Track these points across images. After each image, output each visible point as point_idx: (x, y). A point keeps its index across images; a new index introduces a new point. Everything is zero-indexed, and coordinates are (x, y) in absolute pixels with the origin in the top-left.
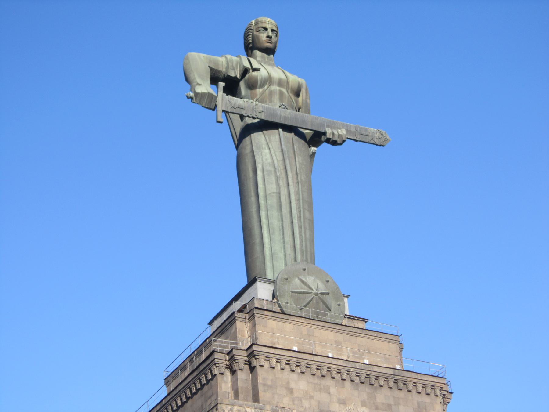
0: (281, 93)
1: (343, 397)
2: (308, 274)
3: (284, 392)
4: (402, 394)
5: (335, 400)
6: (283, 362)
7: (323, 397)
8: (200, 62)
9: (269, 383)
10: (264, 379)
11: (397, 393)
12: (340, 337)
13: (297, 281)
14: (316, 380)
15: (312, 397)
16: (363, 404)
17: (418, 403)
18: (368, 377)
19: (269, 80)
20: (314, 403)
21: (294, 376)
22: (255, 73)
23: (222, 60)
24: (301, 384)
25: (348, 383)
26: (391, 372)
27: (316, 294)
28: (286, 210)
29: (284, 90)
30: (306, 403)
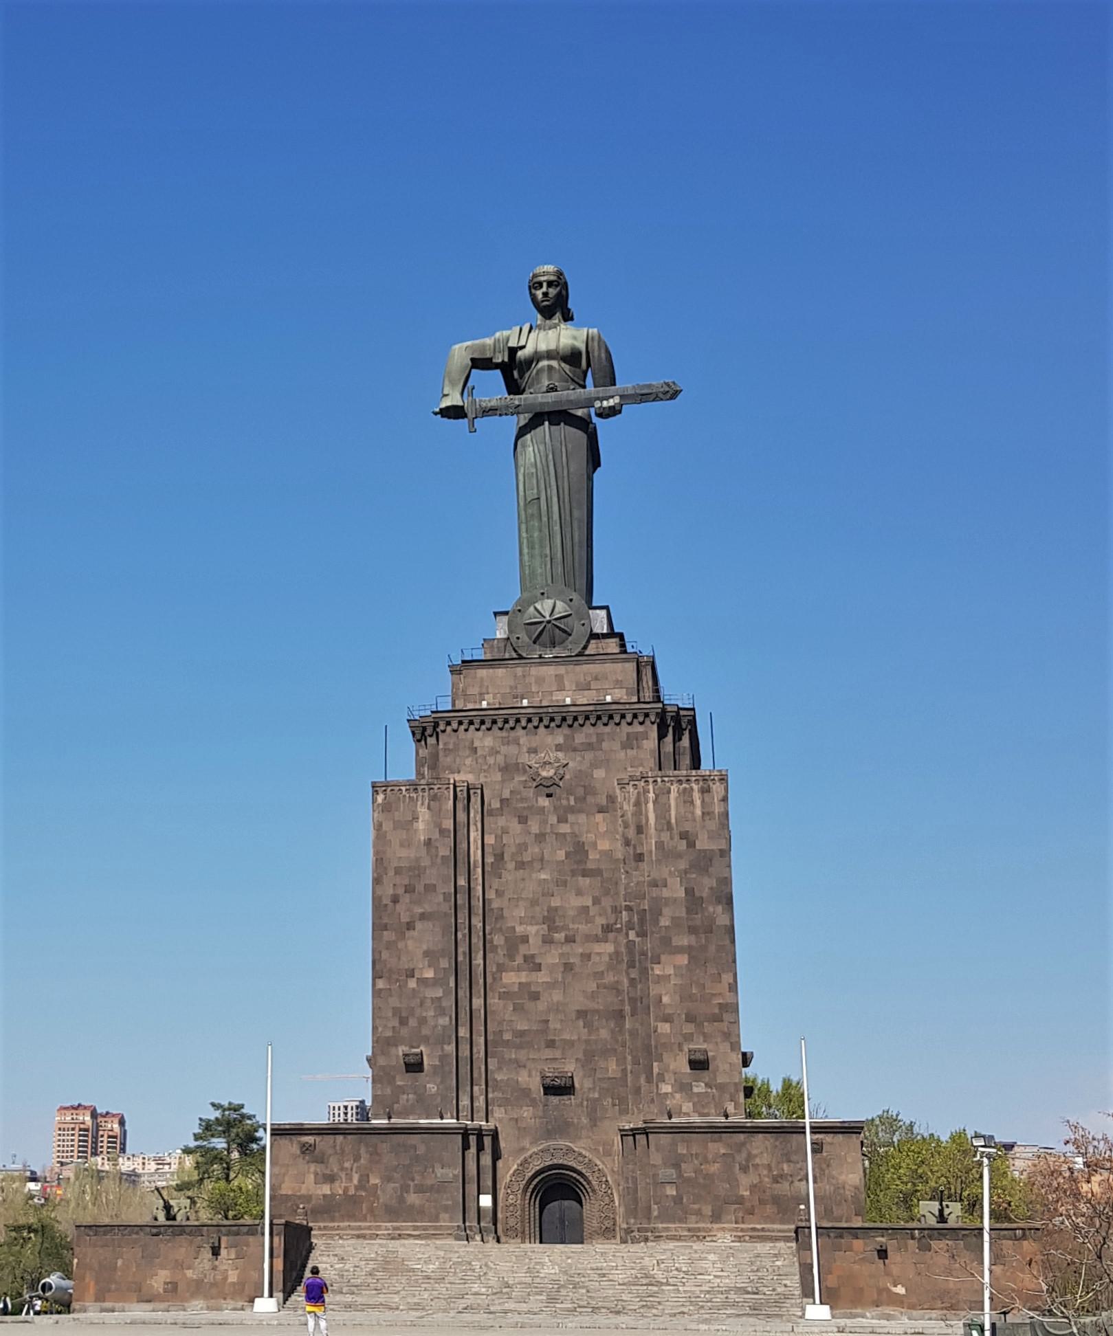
0: (550, 368)
1: (534, 745)
2: (548, 598)
3: (468, 752)
4: (607, 729)
5: (525, 749)
6: (466, 722)
7: (513, 749)
8: (460, 353)
9: (451, 747)
10: (445, 744)
11: (600, 728)
12: (561, 670)
13: (532, 609)
14: (504, 734)
15: (498, 752)
16: (559, 748)
17: (628, 734)
18: (564, 719)
19: (537, 357)
20: (500, 759)
21: (480, 733)
22: (520, 353)
23: (489, 341)
24: (485, 740)
25: (542, 729)
26: (591, 708)
27: (549, 622)
28: (545, 519)
29: (554, 363)
30: (491, 760)
